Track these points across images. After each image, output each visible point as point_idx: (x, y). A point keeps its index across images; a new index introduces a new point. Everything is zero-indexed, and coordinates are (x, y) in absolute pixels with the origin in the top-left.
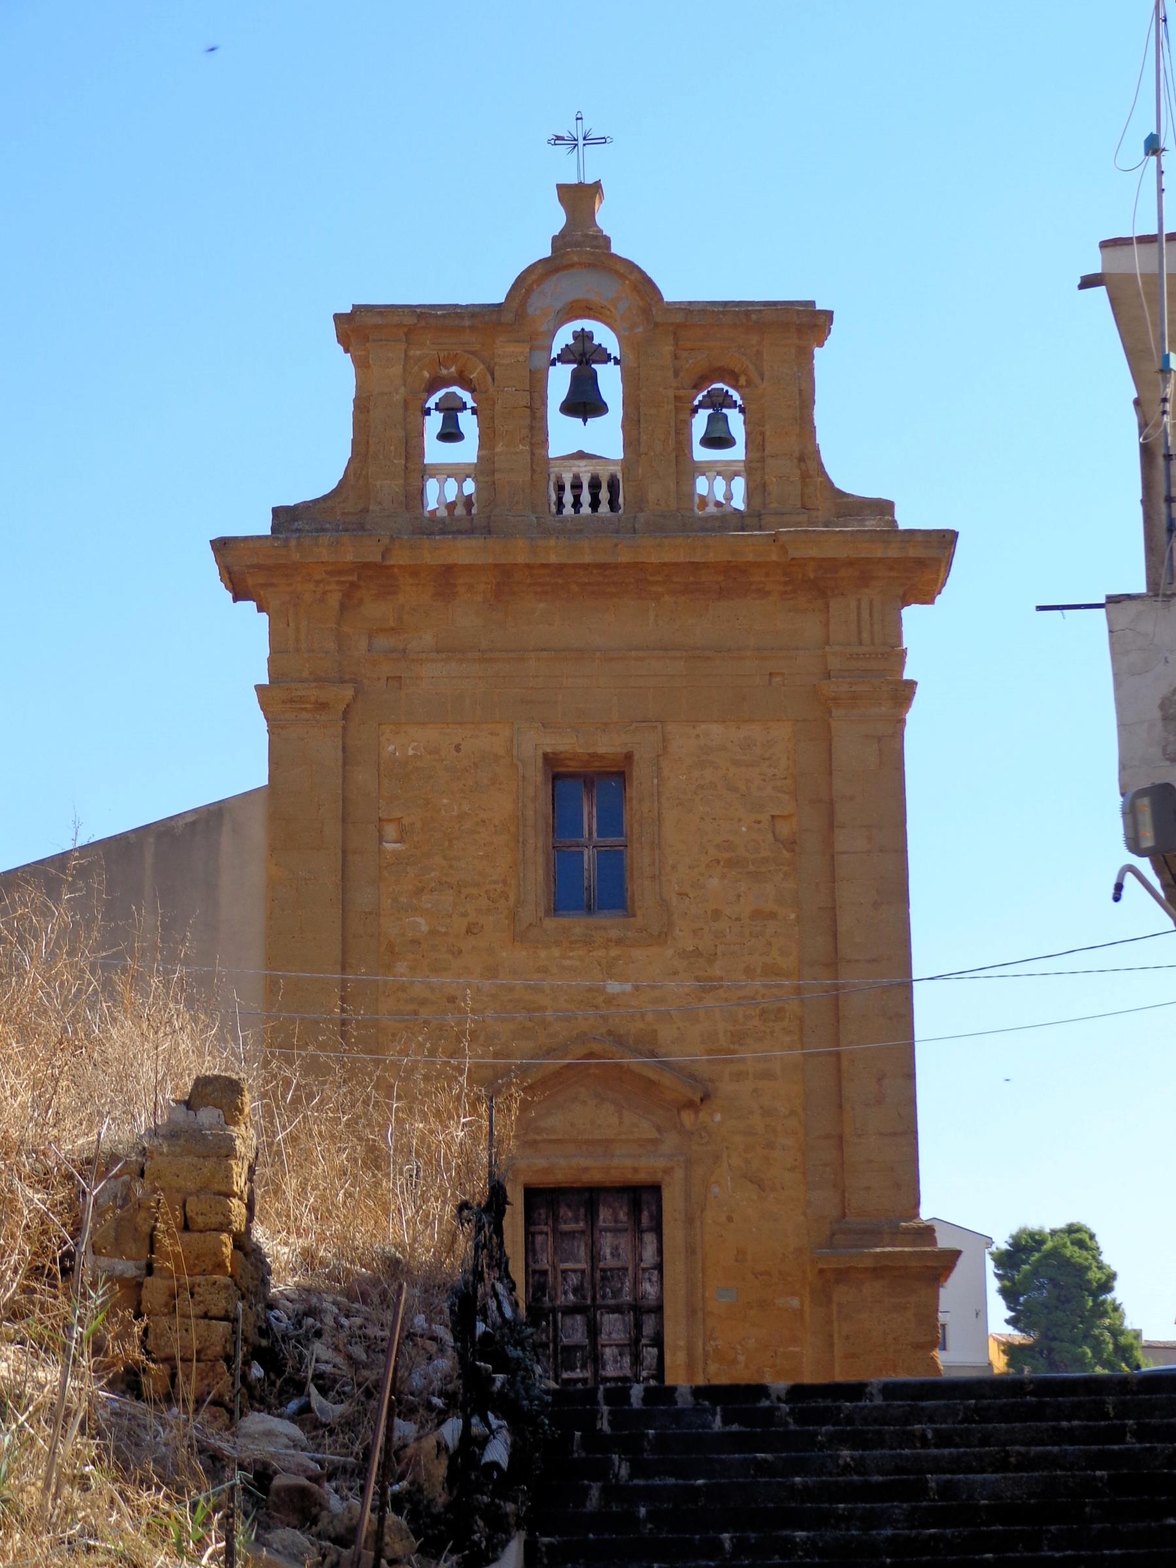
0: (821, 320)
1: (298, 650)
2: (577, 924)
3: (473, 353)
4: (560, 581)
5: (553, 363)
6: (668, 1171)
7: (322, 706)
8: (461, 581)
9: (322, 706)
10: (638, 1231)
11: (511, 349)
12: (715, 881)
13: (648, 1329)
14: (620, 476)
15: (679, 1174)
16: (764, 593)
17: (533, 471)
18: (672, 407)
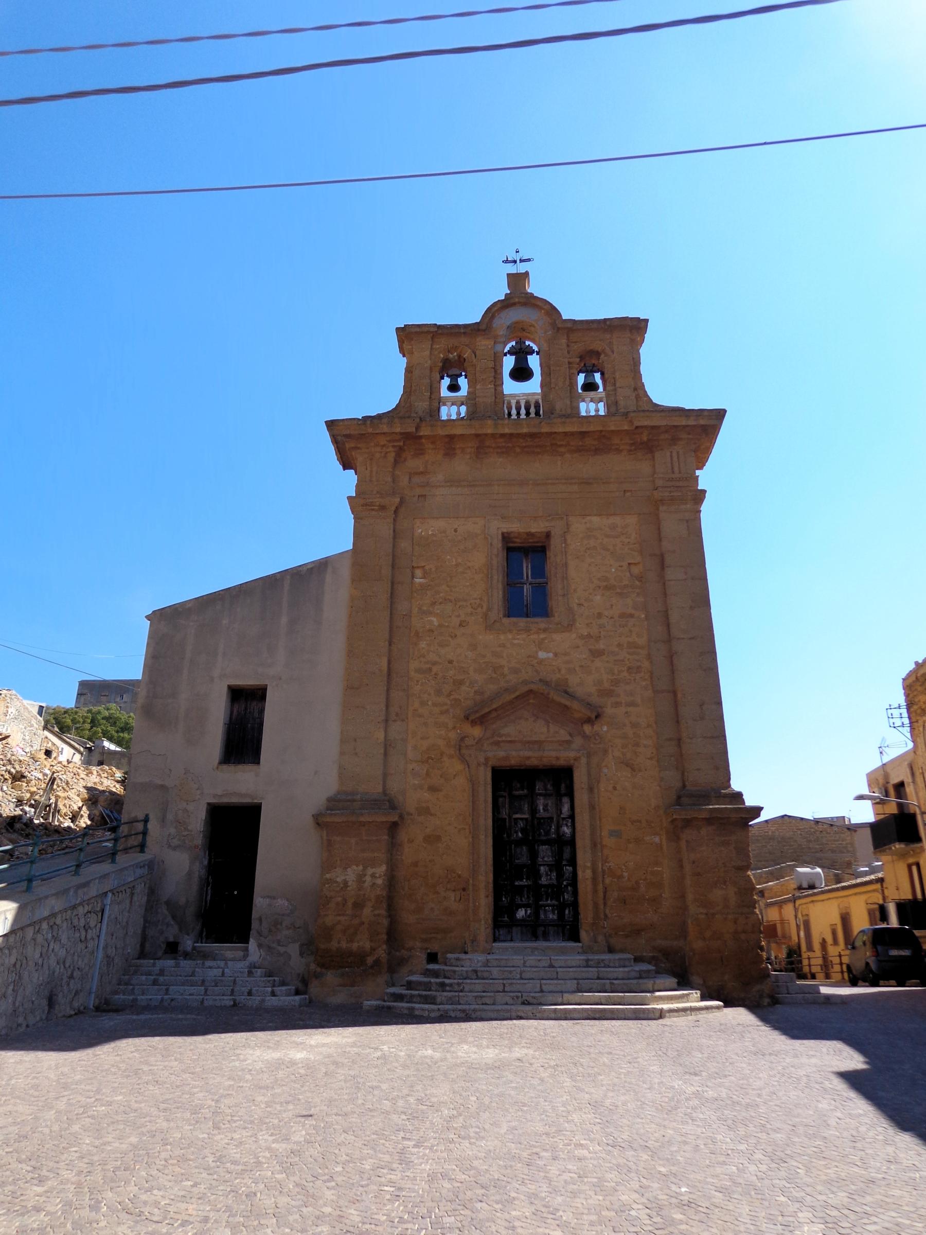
0: (643, 324)
1: (371, 481)
2: (522, 622)
3: (466, 345)
4: (510, 445)
5: (505, 355)
6: (576, 759)
7: (383, 508)
8: (458, 446)
9: (383, 508)
10: (559, 796)
11: (484, 342)
12: (598, 597)
13: (567, 855)
14: (540, 402)
15: (584, 760)
16: (619, 451)
17: (496, 397)
18: (567, 366)
